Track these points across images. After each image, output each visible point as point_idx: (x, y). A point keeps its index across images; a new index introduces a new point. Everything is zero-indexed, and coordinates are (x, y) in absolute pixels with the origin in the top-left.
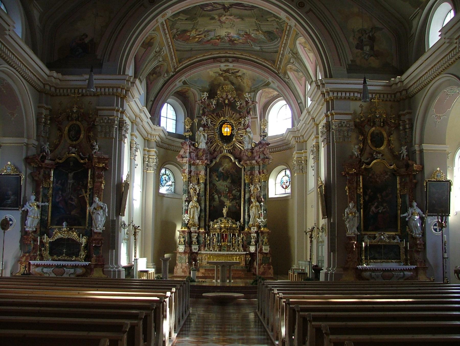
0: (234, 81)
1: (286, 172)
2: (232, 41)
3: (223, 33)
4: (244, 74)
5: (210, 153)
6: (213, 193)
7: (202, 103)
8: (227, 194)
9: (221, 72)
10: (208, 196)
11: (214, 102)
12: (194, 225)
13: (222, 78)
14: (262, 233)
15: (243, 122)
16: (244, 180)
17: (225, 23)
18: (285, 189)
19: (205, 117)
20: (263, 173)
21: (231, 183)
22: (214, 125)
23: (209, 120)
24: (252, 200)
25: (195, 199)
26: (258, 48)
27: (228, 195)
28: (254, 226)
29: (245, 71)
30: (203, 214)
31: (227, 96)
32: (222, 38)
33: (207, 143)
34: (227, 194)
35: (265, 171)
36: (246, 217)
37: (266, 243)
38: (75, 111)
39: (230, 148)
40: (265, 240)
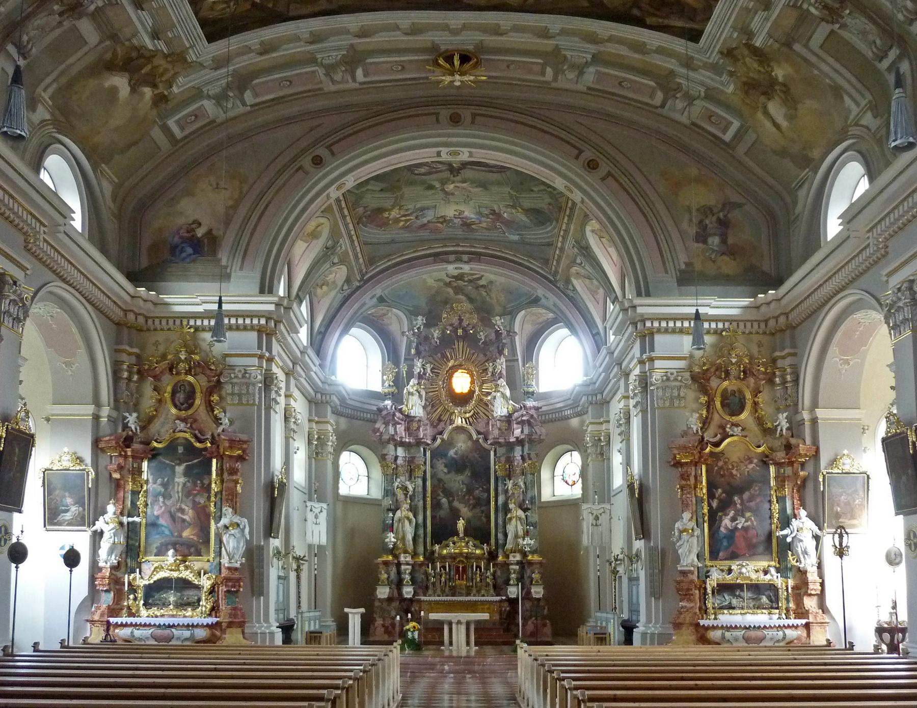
0: (474, 294)
2: (467, 225)
3: (450, 211)
5: (432, 424)
9: (448, 280)
10: (429, 499)
11: (436, 333)
12: (406, 552)
13: (450, 290)
15: (491, 369)
16: (495, 472)
17: (453, 194)
20: (530, 459)
22: (437, 374)
24: (512, 506)
25: (405, 506)
26: (516, 238)
29: (492, 277)
30: (421, 532)
31: (461, 320)
32: (451, 220)
33: (424, 408)
34: (464, 496)
38: (183, 357)
39: (468, 415)
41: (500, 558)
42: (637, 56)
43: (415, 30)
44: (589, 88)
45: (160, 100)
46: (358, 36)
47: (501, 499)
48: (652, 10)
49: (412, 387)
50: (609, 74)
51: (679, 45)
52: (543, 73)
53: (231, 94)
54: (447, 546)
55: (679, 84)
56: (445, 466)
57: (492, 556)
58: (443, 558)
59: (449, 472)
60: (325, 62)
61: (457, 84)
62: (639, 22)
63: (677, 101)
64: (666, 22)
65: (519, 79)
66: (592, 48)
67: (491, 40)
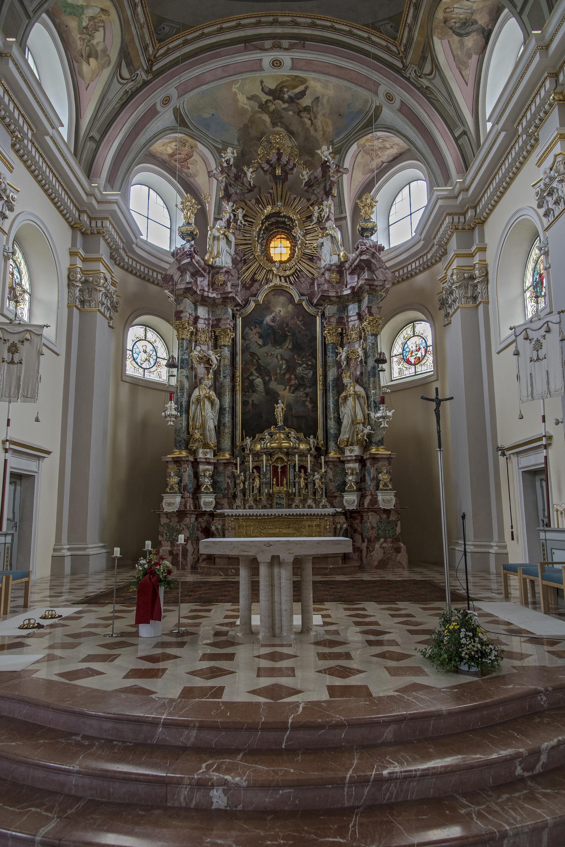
1: (414, 327)
4: (317, 99)
6: (252, 374)
7: (222, 172)
8: (284, 374)
10: (239, 379)
12: (206, 445)
13: (266, 118)
14: (375, 459)
15: (316, 215)
16: (324, 338)
18: (415, 365)
19: (231, 204)
21: (292, 350)
23: (240, 210)
27: (287, 376)
28: (352, 444)
30: (227, 419)
34: (284, 374)
35: (374, 310)
36: (332, 423)
37: (385, 485)
39: (288, 273)
40: (384, 477)
41: (332, 454)
47: (332, 374)
49: (218, 230)
54: (262, 439)
56: (261, 337)
57: (321, 451)
58: (257, 455)
59: (265, 345)
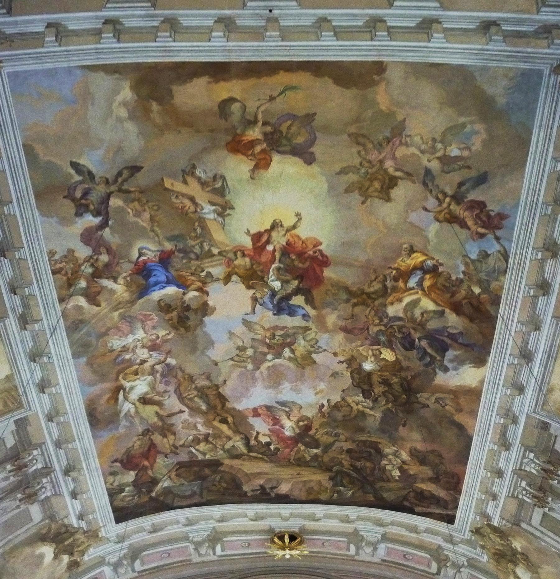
42: (414, 535)
43: (257, 518)
44: (383, 561)
45: (74, 565)
46: (220, 521)
48: (417, 502)
50: (395, 549)
51: (441, 527)
52: (348, 549)
53: (125, 562)
55: (447, 556)
60: (195, 540)
61: (288, 557)
62: (411, 511)
63: (449, 569)
64: (428, 510)
65: (332, 554)
66: (381, 530)
67: (310, 525)
